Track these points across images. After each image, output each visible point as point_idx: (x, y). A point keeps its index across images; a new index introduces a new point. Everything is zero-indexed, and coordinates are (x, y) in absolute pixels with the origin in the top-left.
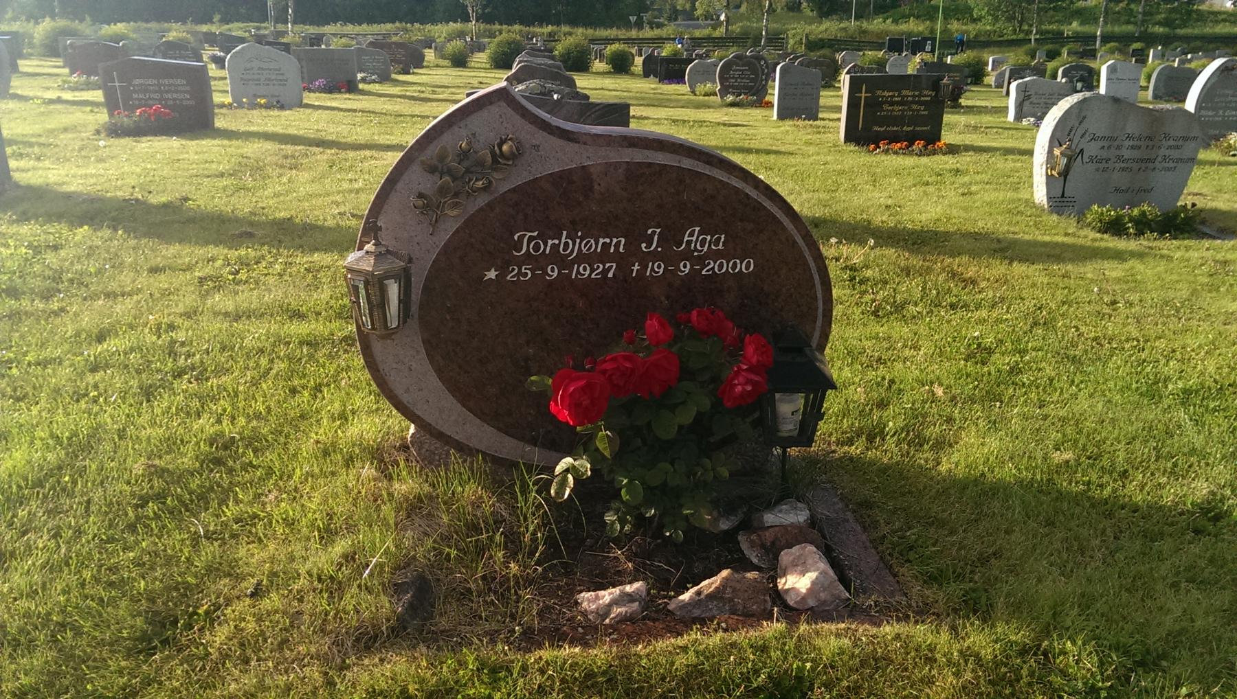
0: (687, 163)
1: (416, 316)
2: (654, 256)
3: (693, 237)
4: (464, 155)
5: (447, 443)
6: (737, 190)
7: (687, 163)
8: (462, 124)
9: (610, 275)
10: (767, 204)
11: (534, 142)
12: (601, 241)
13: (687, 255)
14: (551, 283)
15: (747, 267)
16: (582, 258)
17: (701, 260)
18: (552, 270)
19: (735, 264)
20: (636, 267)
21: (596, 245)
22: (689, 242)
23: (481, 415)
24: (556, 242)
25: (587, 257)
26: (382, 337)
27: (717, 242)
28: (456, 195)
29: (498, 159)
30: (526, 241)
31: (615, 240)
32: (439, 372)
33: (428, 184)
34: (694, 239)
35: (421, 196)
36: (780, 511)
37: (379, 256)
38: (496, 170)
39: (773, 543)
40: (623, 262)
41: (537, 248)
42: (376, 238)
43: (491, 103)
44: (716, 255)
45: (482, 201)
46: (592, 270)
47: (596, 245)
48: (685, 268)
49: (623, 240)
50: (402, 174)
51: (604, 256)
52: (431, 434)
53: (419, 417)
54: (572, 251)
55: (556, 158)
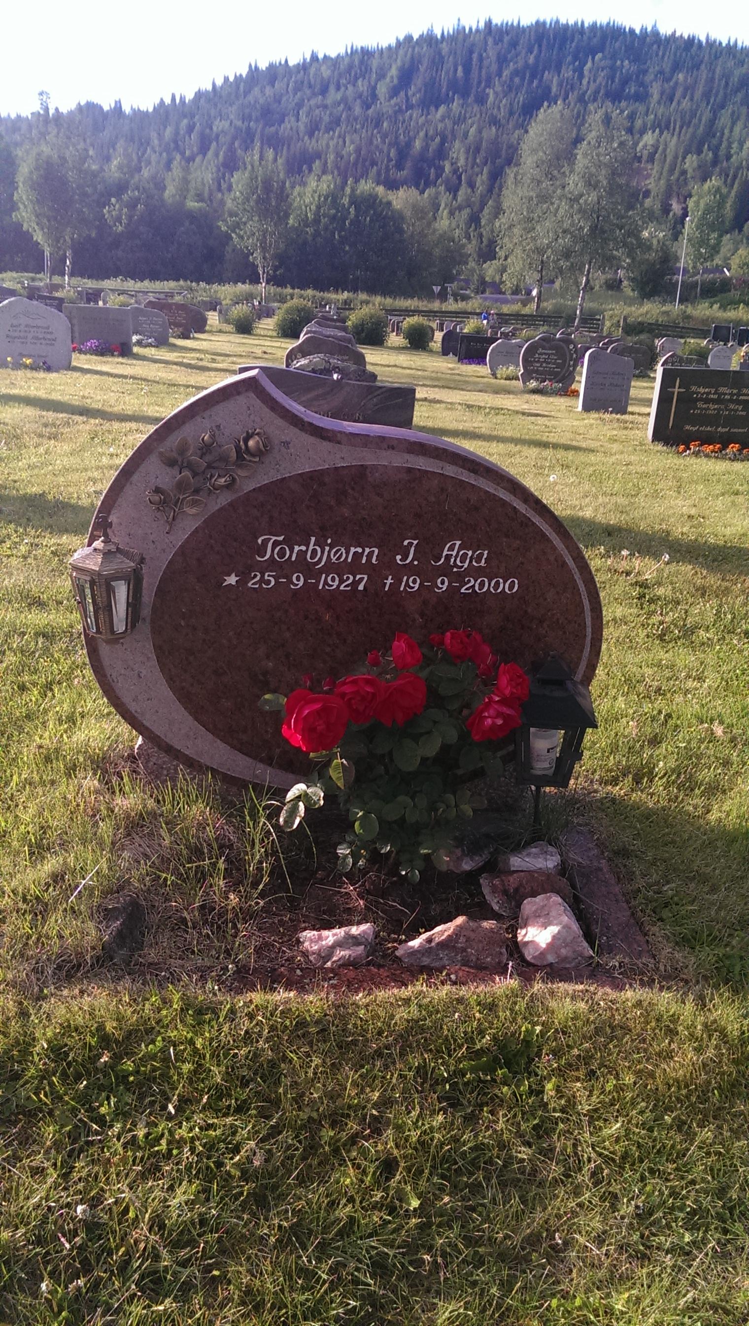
0: (450, 470)
1: (148, 620)
2: (410, 569)
3: (453, 551)
4: (206, 449)
5: (177, 758)
6: (504, 503)
7: (450, 470)
8: (208, 413)
9: (361, 587)
10: (537, 520)
11: (284, 438)
12: (353, 550)
13: (446, 570)
16: (330, 567)
17: (460, 578)
18: (298, 579)
19: (498, 583)
20: (389, 581)
21: (347, 554)
22: (448, 557)
23: (214, 730)
24: (304, 548)
25: (335, 564)
26: (108, 642)
28: (197, 491)
30: (271, 545)
31: (367, 550)
32: (171, 681)
33: (166, 478)
34: (454, 553)
35: (157, 490)
36: (528, 855)
37: (107, 554)
38: (240, 466)
39: (517, 890)
41: (282, 554)
42: (106, 535)
43: (239, 393)
44: (477, 573)
45: (224, 500)
46: (341, 581)
47: (347, 554)
48: (443, 585)
49: (376, 551)
50: (138, 466)
51: (355, 566)
52: (160, 747)
53: (147, 728)
55: (305, 457)
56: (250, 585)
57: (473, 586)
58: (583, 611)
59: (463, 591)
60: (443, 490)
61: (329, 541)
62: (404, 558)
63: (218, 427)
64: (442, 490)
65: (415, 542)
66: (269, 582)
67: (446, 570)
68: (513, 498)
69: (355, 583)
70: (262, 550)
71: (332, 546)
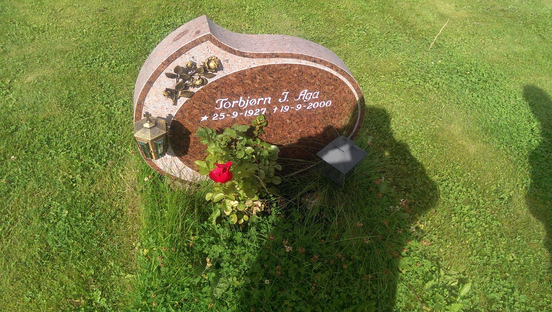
2: (285, 103)
3: (304, 94)
6: (327, 73)
7: (304, 62)
9: (263, 113)
10: (341, 77)
14: (234, 119)
16: (249, 108)
17: (307, 103)
19: (323, 103)
22: (302, 97)
24: (237, 102)
29: (206, 70)
30: (222, 102)
31: (266, 99)
33: (171, 84)
34: (304, 95)
35: (167, 90)
40: (269, 107)
44: (315, 100)
46: (254, 112)
47: (255, 101)
48: (299, 107)
49: (270, 98)
51: (261, 105)
54: (245, 105)
56: (213, 119)
59: (308, 108)
60: (300, 71)
61: (249, 97)
63: (193, 57)
64: (300, 71)
66: (222, 117)
67: (301, 102)
68: (331, 70)
70: (218, 105)
71: (250, 100)
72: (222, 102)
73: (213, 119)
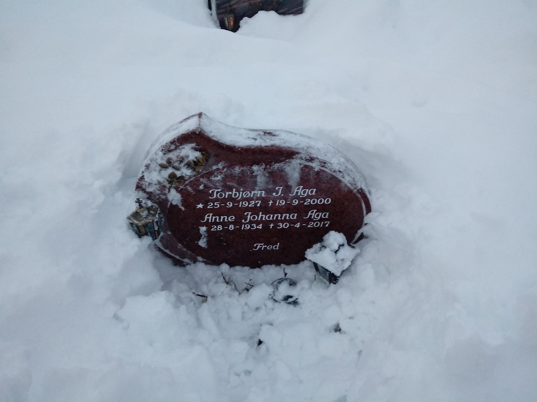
2: (280, 198)
9: (258, 205)
15: (328, 201)
16: (243, 199)
18: (230, 204)
20: (271, 202)
22: (297, 192)
24: (231, 193)
27: (312, 192)
41: (221, 195)
44: (310, 197)
46: (249, 204)
56: (208, 207)
57: (310, 202)
58: (362, 208)
59: (305, 204)
62: (277, 193)
65: (282, 188)
66: (217, 206)
69: (256, 204)
71: (243, 192)
72: (215, 192)
73: (208, 207)
